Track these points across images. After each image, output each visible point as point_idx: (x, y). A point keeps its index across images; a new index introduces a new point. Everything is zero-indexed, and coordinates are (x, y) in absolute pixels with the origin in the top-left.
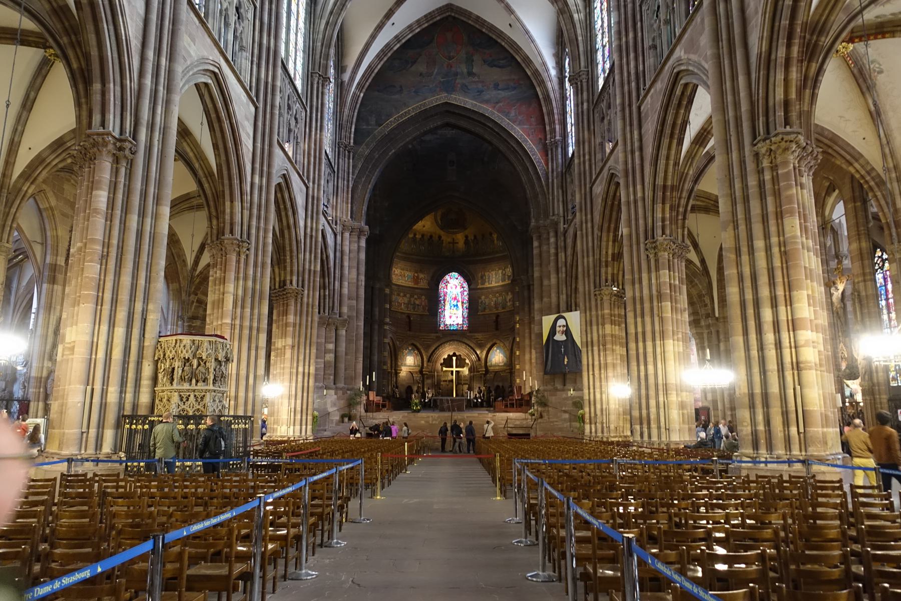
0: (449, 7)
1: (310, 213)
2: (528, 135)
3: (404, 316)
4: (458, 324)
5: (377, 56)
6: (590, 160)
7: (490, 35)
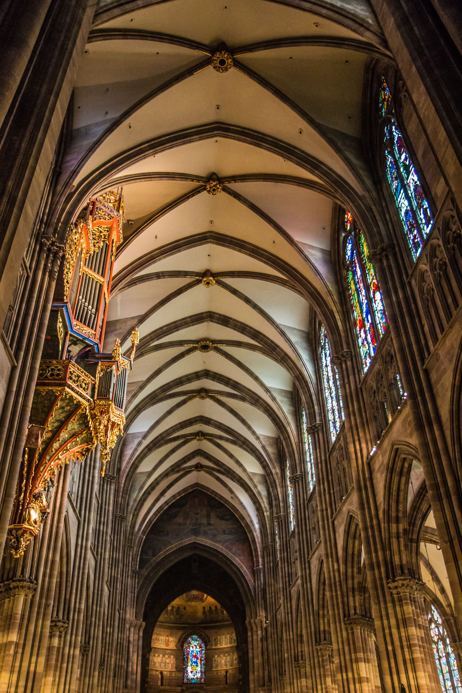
0: (197, 484)
1: (120, 629)
2: (243, 563)
3: (158, 673)
4: (197, 678)
5: (154, 514)
6: (275, 596)
7: (221, 501)
